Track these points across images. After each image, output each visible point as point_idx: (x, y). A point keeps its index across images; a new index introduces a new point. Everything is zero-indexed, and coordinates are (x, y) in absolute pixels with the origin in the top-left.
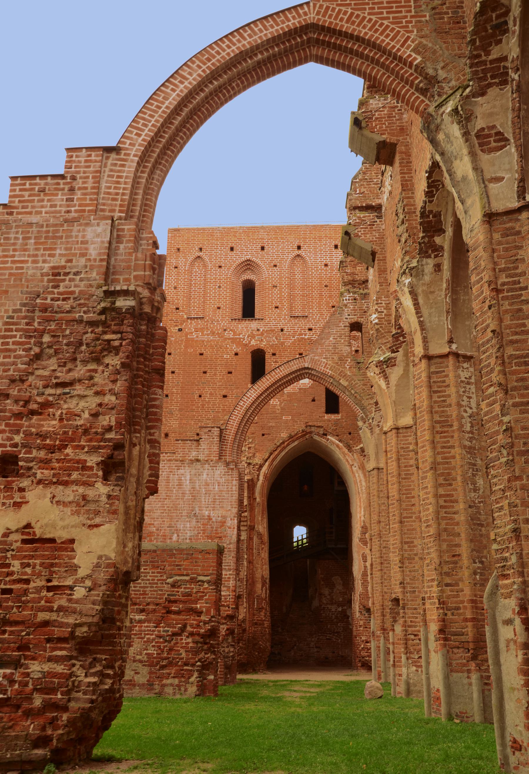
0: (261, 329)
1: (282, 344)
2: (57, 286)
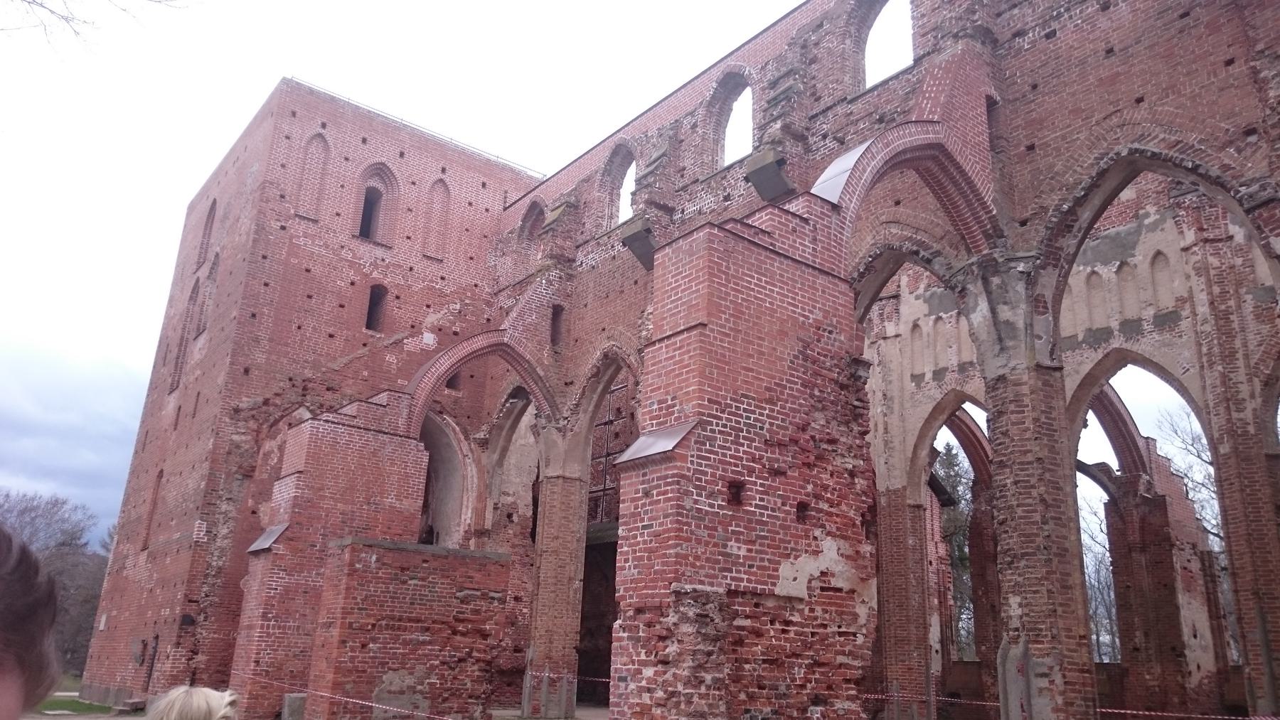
0: (387, 261)
1: (409, 287)
2: (819, 341)
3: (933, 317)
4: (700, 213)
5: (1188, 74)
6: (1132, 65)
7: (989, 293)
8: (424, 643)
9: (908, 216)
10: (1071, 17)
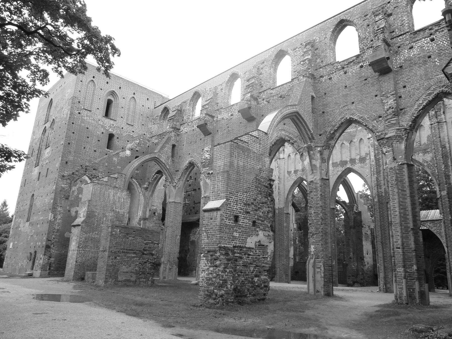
1: (122, 134)
2: (260, 174)
3: (295, 153)
4: (223, 119)
5: (366, 97)
6: (352, 92)
7: (310, 156)
8: (134, 257)
10: (336, 74)
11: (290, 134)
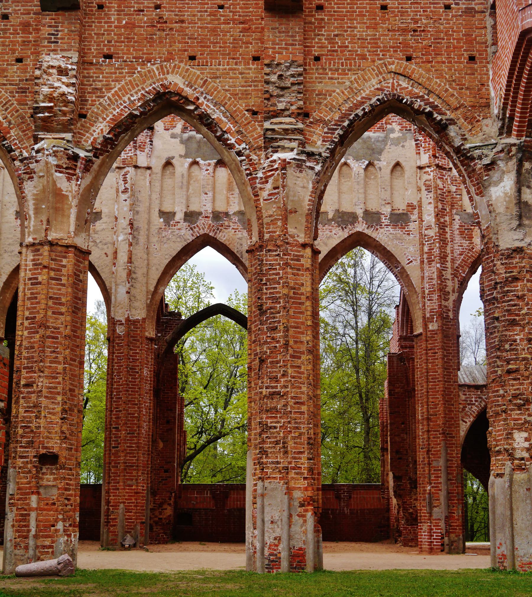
3: (190, 160)
7: (519, 172)
9: (421, 75)
11: (430, 92)
